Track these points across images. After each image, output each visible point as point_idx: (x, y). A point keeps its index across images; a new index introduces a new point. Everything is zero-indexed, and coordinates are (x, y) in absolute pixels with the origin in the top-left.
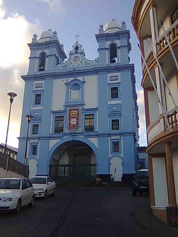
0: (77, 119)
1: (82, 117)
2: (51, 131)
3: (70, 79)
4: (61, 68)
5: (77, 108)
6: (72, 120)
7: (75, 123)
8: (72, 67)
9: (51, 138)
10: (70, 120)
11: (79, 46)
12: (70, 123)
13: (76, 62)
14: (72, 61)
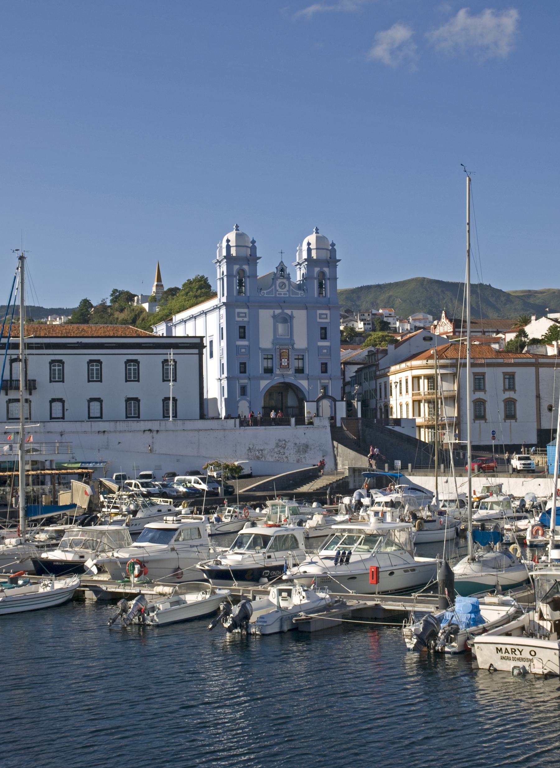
0: (288, 360)
1: (292, 357)
2: (261, 371)
3: (278, 311)
4: (265, 295)
5: (287, 347)
6: (283, 360)
7: (286, 364)
8: (278, 296)
9: (263, 379)
10: (281, 360)
11: (284, 268)
12: (281, 364)
13: (282, 289)
14: (278, 288)
